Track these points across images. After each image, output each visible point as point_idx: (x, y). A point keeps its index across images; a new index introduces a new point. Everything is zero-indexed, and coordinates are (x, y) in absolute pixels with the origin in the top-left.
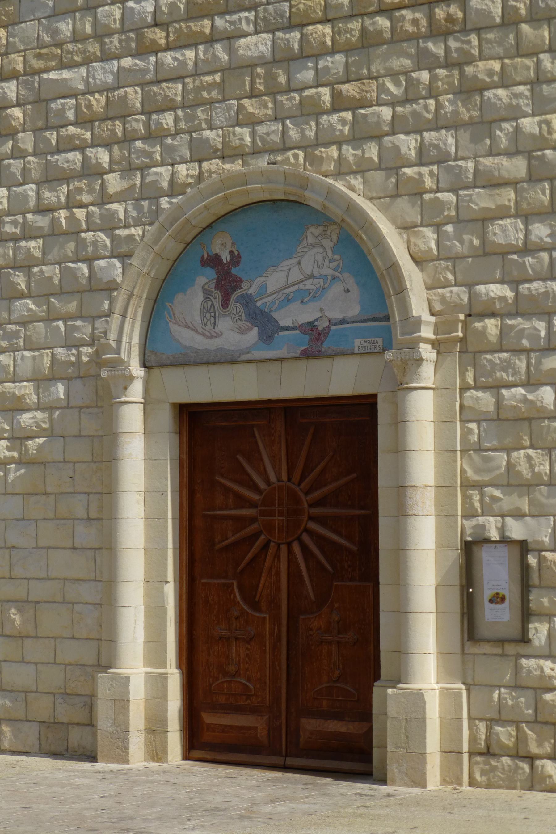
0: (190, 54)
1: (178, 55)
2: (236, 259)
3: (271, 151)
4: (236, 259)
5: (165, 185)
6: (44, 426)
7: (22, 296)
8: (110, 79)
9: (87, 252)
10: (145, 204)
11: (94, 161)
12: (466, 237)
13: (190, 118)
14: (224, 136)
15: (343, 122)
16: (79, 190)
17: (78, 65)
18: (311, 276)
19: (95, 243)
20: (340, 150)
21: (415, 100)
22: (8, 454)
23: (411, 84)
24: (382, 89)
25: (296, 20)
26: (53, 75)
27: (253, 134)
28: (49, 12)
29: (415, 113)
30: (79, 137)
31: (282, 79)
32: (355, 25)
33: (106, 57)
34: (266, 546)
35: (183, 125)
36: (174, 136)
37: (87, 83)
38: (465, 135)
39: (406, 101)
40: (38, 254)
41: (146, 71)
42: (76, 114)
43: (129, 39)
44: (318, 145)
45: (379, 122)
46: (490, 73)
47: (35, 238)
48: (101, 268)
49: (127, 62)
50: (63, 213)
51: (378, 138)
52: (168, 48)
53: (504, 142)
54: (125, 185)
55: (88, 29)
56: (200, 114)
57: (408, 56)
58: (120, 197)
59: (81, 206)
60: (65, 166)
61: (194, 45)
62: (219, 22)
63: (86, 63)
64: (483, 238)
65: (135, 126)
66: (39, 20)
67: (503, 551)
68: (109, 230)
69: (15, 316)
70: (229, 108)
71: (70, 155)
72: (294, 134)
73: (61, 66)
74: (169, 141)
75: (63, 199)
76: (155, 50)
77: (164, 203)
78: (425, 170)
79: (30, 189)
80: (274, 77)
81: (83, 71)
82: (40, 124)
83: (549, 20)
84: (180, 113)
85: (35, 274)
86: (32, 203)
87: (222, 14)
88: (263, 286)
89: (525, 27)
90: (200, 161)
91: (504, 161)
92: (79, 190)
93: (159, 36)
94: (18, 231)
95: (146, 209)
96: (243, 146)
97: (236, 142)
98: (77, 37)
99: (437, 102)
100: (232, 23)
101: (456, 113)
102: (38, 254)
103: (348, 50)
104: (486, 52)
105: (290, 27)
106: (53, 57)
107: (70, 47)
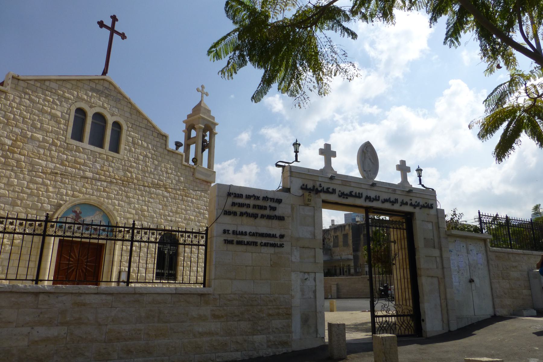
0: (74, 170)
1: (72, 169)
2: (80, 213)
3: (90, 195)
4: (80, 213)
5: (65, 194)
6: (20, 238)
7: (18, 206)
8: (53, 167)
9: (42, 201)
10: (59, 196)
11: (46, 183)
12: (125, 220)
13: (72, 182)
14: (79, 189)
15: (106, 195)
16: (41, 187)
17: (44, 161)
18: (97, 220)
19: (44, 200)
20: (104, 199)
21: (118, 196)
22: (7, 243)
23: (118, 192)
24: (113, 192)
25: (99, 174)
26: (37, 160)
27: (86, 190)
28: (37, 146)
29: (118, 198)
30: (42, 176)
31: (94, 183)
32: (109, 179)
33: (52, 162)
34: (73, 270)
35: (70, 183)
36: (68, 184)
37: (46, 165)
38: (126, 204)
39: (116, 195)
40: (26, 198)
41: (63, 169)
42: (41, 171)
43: (59, 161)
44: (99, 197)
45: (112, 197)
46: (132, 196)
47: (25, 194)
48: (45, 206)
49: (58, 165)
50: (36, 191)
51: (111, 200)
52: (69, 167)
53: (132, 207)
54: (54, 190)
55: (48, 155)
56: (75, 182)
57: (118, 188)
58: (52, 192)
59: (41, 191)
60: (38, 181)
61: (75, 169)
62: (82, 167)
63: (47, 161)
64: (127, 221)
65: (58, 179)
66: (33, 146)
67: (125, 273)
68: (48, 199)
69: (15, 210)
70: (81, 184)
71: (39, 179)
72: (95, 193)
73: (39, 159)
74: (66, 185)
75: (35, 188)
76: (65, 166)
77: (64, 197)
78: (119, 208)
79: (26, 183)
80: (93, 182)
81: (46, 162)
82: (30, 168)
83: (141, 191)
84: (70, 180)
85: (24, 202)
86: (25, 186)
87: (82, 166)
88: (86, 220)
89: (137, 191)
90: (73, 192)
91: (132, 210)
92: (41, 187)
93: (67, 164)
94: (20, 191)
95: (59, 197)
96: (84, 192)
97: (83, 191)
98: (44, 154)
99: (122, 197)
100: (85, 168)
101: (125, 200)
102: (26, 198)
103: (107, 182)
104: (131, 192)
105: (97, 174)
106: (37, 156)
107: (43, 156)
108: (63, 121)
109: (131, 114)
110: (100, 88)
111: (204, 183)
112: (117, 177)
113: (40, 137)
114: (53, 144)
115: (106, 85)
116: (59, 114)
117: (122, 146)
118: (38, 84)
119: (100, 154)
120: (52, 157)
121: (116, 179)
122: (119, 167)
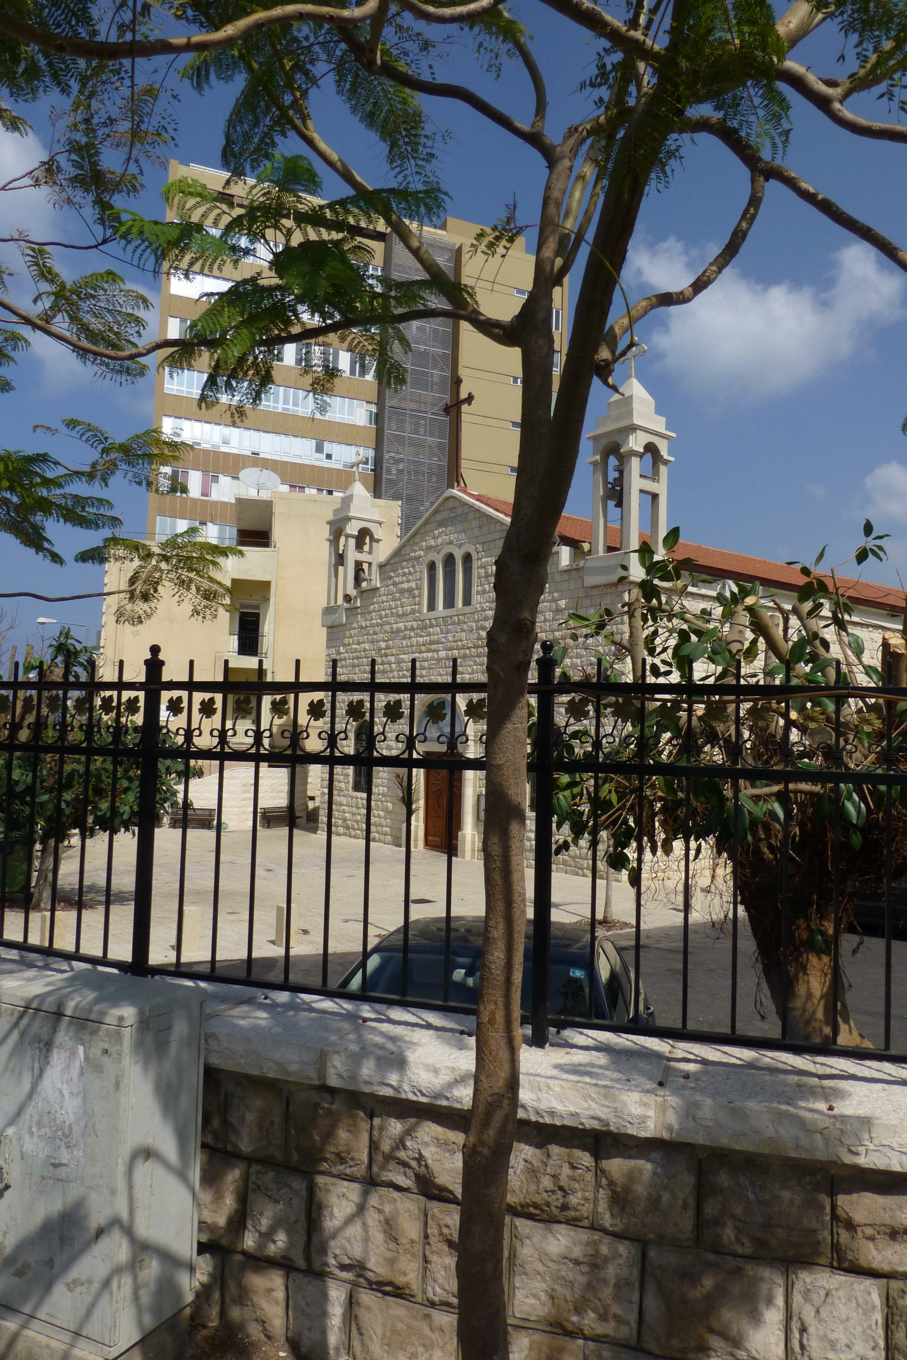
93: (423, 648)
108: (416, 592)
109: (480, 527)
110: (445, 514)
111: (609, 590)
112: (470, 645)
113: (401, 625)
114: (412, 629)
115: (451, 504)
116: (413, 585)
117: (475, 589)
118: (397, 559)
119: (451, 617)
120: (412, 646)
121: (469, 648)
122: (471, 627)
